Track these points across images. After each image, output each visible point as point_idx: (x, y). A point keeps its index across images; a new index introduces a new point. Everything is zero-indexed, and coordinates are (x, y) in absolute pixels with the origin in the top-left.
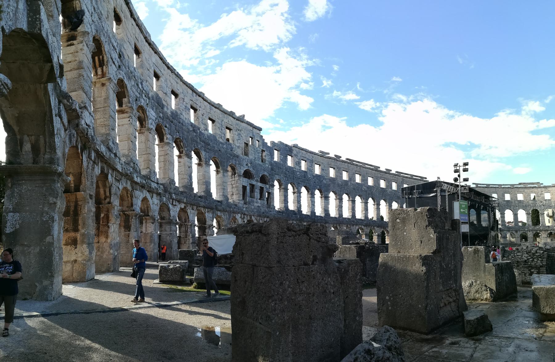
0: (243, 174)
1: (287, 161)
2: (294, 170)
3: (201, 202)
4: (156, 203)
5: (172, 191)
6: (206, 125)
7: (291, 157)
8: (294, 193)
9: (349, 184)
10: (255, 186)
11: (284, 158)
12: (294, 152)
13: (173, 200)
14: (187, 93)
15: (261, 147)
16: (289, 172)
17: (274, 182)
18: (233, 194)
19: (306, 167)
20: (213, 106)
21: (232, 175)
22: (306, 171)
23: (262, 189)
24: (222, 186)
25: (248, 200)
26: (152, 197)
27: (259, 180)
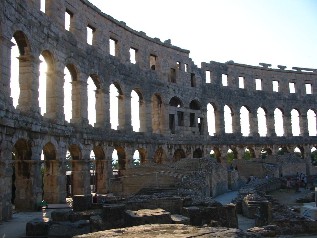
0: (170, 103)
6: (128, 56)
8: (232, 115)
9: (298, 97)
12: (230, 70)
13: (85, 139)
14: (106, 24)
15: (190, 71)
18: (159, 124)
20: (136, 34)
21: (158, 104)
22: (246, 88)
24: (145, 116)
25: (176, 129)
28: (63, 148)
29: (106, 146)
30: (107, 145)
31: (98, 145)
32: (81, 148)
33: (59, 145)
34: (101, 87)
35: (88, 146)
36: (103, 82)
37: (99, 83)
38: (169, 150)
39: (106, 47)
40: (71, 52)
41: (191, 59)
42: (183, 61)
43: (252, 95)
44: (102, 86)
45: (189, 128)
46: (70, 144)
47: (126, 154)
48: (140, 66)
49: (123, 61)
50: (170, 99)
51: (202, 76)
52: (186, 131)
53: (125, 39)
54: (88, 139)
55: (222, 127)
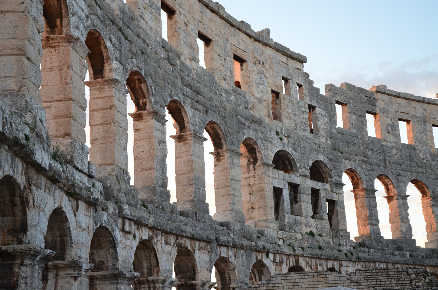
0: (274, 162)
1: (366, 126)
2: (383, 145)
3: (186, 224)
4: (84, 225)
5: (122, 197)
7: (372, 116)
8: (389, 198)
10: (301, 187)
11: (358, 119)
12: (380, 104)
13: (124, 218)
16: (372, 150)
17: (340, 177)
18: (252, 208)
19: (411, 136)
21: (249, 163)
22: (413, 143)
23: (315, 193)
25: (287, 220)
26: (76, 210)
27: (308, 173)
28: (83, 230)
29: (161, 243)
30: (163, 242)
34: (148, 106)
37: (145, 97)
38: (277, 268)
39: (156, 20)
41: (307, 75)
42: (294, 77)
43: (426, 158)
44: (150, 102)
45: (312, 221)
46: (96, 225)
48: (216, 78)
49: (185, 59)
50: (273, 153)
51: (329, 113)
52: (306, 226)
55: (374, 223)
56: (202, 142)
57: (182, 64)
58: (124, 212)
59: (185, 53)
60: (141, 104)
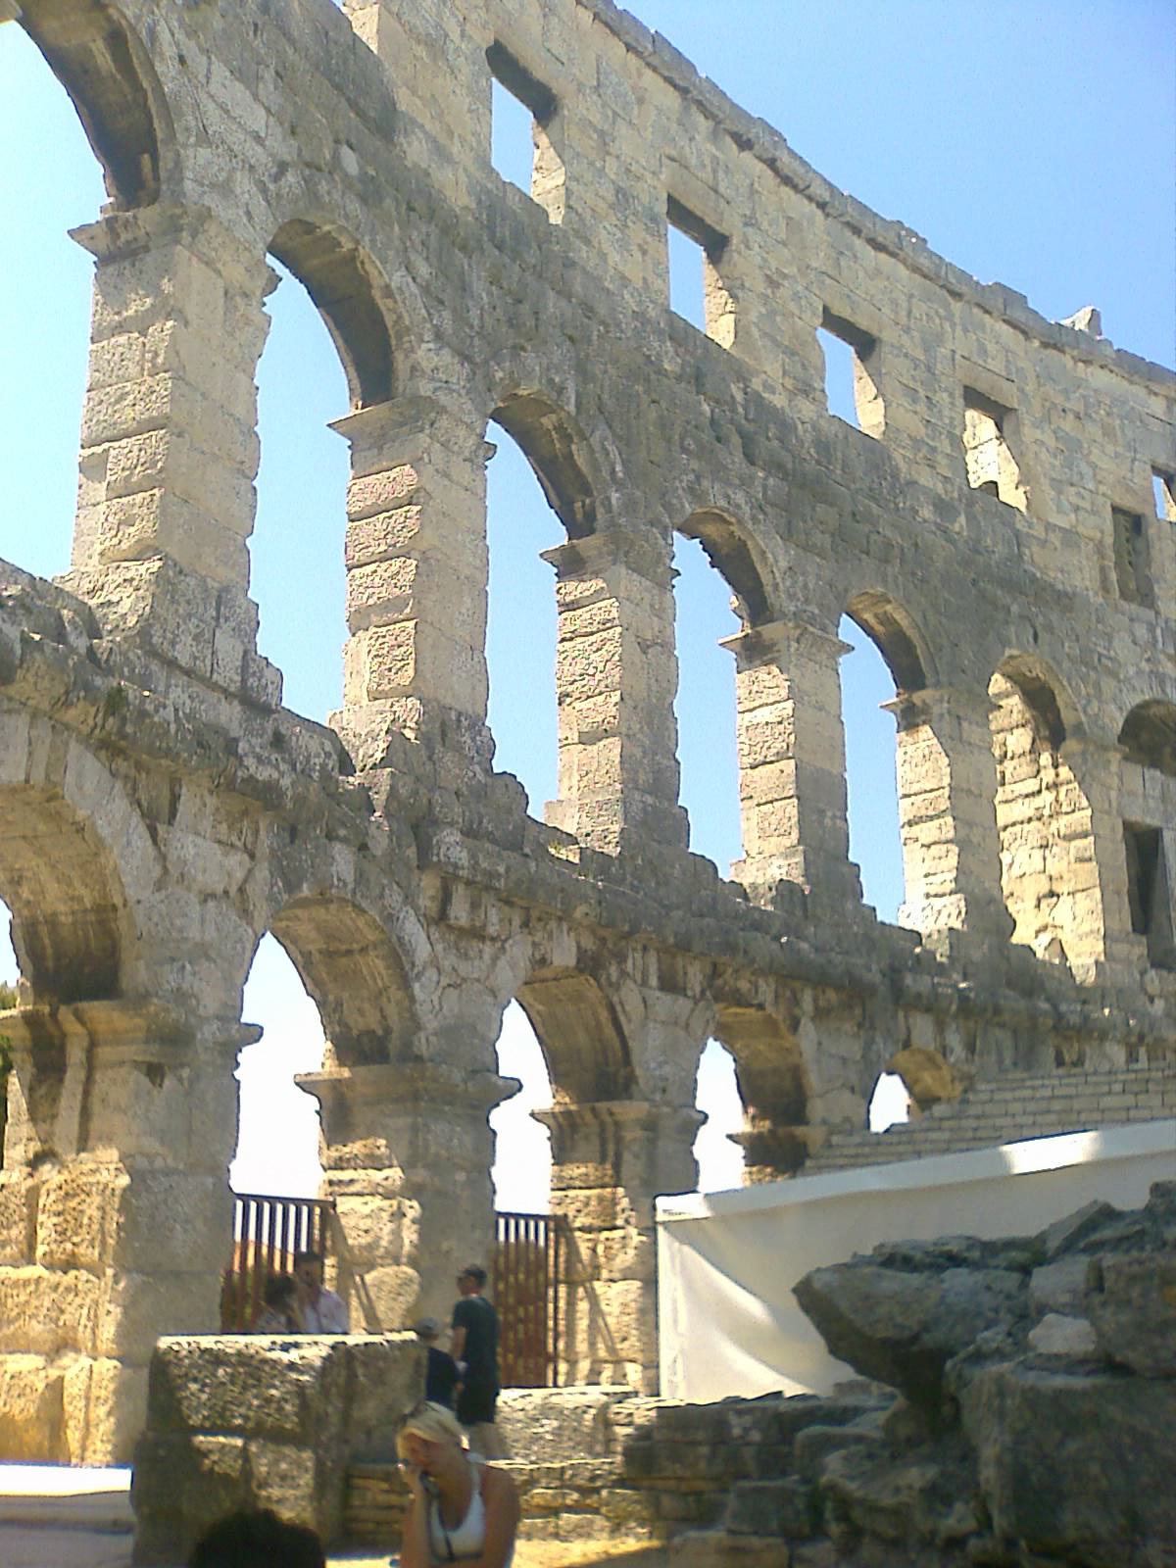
18: (1052, 894)
26: (158, 817)
28: (207, 897)
29: (644, 983)
30: (654, 981)
31: (572, 962)
32: (410, 953)
33: (163, 858)
35: (476, 944)
36: (619, 485)
40: (337, 141)
44: (609, 509)
47: (813, 1080)
53: (784, 244)
54: (482, 886)
56: (833, 657)
57: (755, 400)
58: (438, 855)
59: (767, 368)
60: (579, 517)
